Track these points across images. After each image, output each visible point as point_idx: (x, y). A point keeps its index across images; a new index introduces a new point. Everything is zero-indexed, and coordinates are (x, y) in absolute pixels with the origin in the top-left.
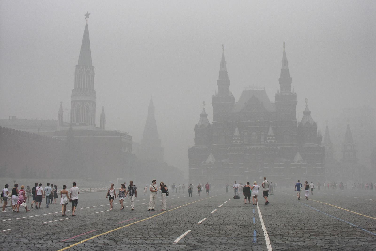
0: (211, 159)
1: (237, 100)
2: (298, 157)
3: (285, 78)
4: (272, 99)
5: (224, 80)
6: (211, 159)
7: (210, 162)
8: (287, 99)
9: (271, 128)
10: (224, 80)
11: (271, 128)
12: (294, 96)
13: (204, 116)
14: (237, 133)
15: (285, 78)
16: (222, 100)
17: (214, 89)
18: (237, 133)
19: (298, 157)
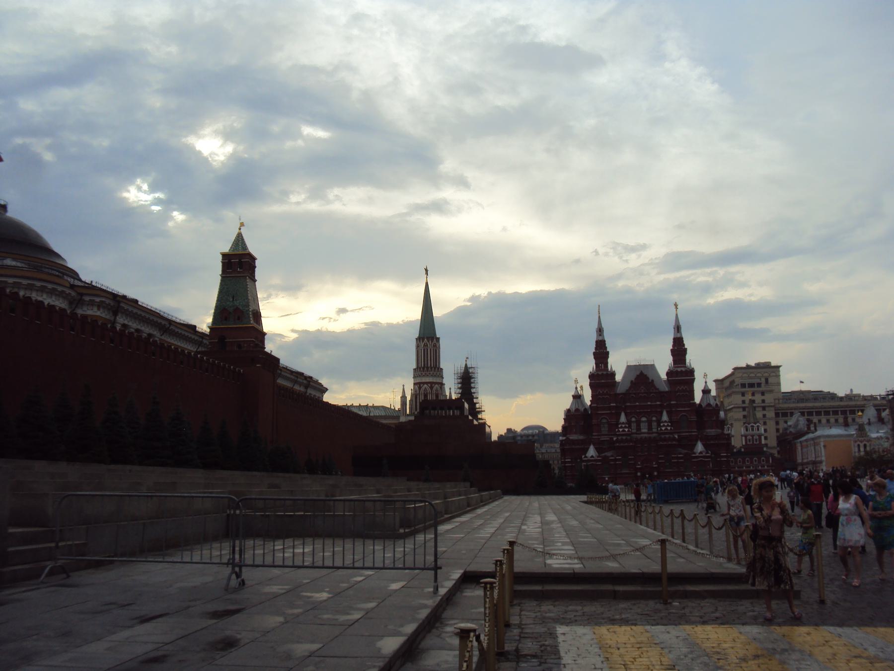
0: (592, 452)
1: (618, 378)
2: (700, 447)
3: (679, 350)
4: (664, 376)
5: (601, 353)
6: (592, 452)
7: (592, 457)
8: (682, 374)
9: (665, 413)
10: (601, 353)
11: (665, 413)
12: (691, 372)
13: (577, 397)
14: (623, 419)
15: (679, 350)
16: (601, 378)
17: (590, 365)
18: (623, 419)
19: (700, 447)
